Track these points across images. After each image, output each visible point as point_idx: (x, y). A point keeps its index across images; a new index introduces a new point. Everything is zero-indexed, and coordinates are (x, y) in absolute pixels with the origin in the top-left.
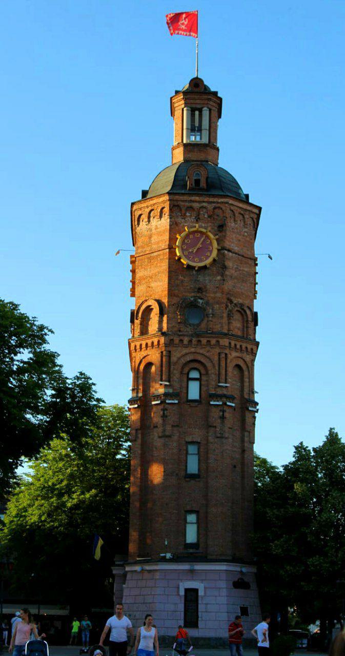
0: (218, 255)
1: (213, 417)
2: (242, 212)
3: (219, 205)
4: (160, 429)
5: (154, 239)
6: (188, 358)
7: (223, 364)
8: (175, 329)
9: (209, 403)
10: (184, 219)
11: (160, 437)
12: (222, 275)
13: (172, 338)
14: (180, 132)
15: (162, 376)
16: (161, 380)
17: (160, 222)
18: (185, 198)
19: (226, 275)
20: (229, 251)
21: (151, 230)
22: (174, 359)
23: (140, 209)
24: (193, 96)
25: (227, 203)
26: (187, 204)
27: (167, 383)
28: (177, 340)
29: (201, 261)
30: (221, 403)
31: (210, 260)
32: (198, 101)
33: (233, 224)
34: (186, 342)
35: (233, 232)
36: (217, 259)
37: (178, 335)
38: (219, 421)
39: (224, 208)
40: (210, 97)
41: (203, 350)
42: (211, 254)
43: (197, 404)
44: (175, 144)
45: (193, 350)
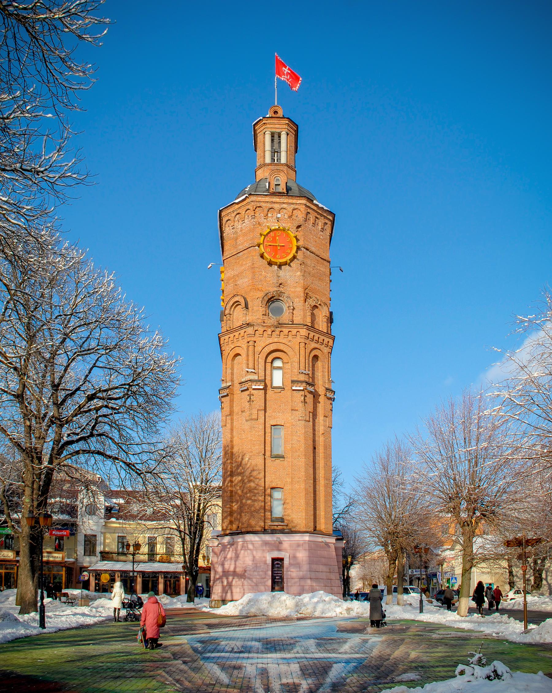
0: (297, 252)
1: (296, 402)
2: (318, 216)
3: (296, 207)
4: (247, 414)
5: (241, 240)
6: (272, 347)
7: (302, 352)
8: (260, 321)
9: (291, 388)
10: (267, 219)
11: (247, 421)
12: (301, 272)
13: (256, 328)
14: (262, 154)
15: (248, 364)
16: (248, 368)
17: (244, 224)
18: (267, 199)
19: (305, 271)
20: (307, 249)
21: (236, 232)
22: (258, 349)
23: (227, 215)
24: (273, 121)
25: (305, 205)
26: (269, 205)
27: (254, 371)
28: (261, 329)
29: (282, 258)
30: (302, 388)
31: (291, 256)
32: (277, 126)
33: (310, 226)
34: (270, 333)
35: (311, 233)
36: (296, 254)
37: (262, 326)
38: (301, 405)
39: (302, 209)
40: (287, 122)
41: (286, 339)
42: (291, 251)
43: (280, 390)
44: (258, 164)
45: (276, 340)
